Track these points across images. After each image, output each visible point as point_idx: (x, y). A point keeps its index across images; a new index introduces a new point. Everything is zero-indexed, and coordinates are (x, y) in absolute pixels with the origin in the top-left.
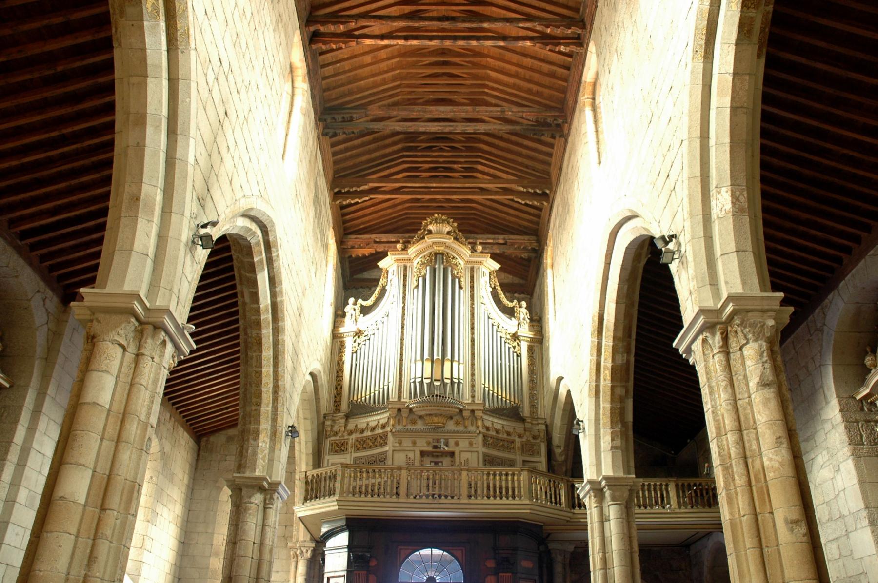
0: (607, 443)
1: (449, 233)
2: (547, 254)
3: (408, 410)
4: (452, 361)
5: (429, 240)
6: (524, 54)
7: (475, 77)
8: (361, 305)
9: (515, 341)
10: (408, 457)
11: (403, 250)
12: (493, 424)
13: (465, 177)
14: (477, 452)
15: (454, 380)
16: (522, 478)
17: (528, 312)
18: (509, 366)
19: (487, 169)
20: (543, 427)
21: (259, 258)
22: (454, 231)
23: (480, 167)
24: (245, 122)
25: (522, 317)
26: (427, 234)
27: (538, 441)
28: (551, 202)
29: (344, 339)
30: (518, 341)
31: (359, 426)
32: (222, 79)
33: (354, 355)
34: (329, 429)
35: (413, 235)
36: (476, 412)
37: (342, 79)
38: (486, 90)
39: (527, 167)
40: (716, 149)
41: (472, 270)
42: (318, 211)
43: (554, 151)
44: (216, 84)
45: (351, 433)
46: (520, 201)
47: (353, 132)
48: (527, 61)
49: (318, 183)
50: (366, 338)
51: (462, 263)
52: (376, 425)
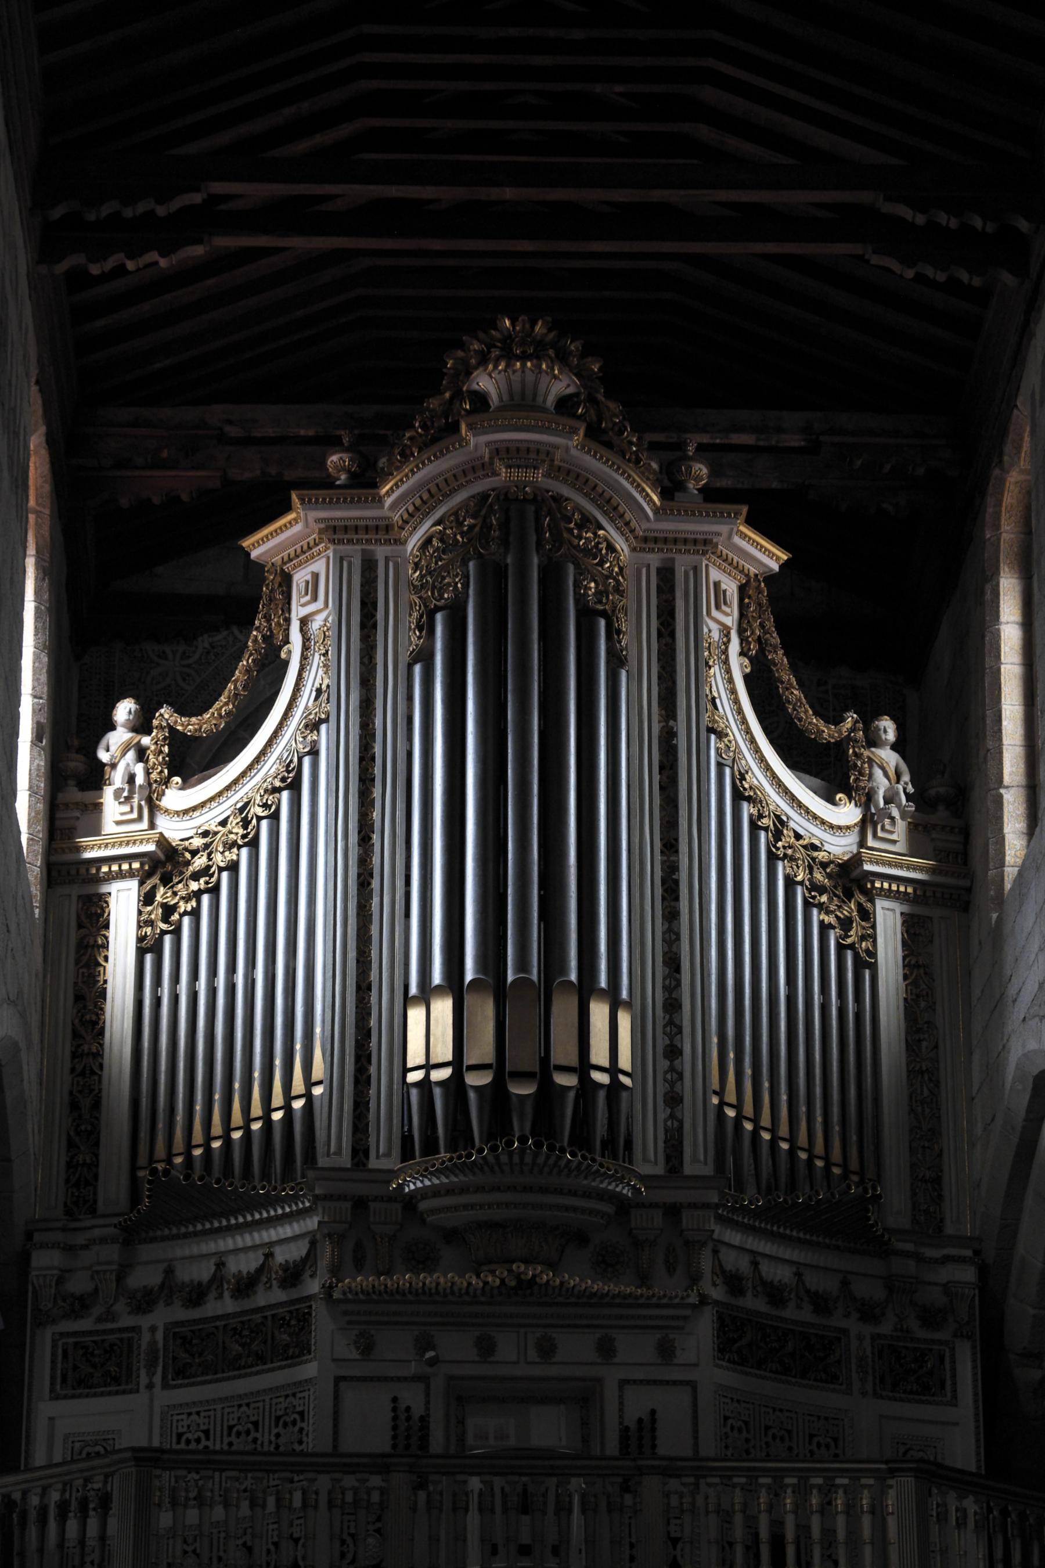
2: (999, 504)
4: (586, 990)
8: (172, 729)
9: (849, 895)
10: (403, 1406)
12: (755, 1264)
14: (693, 1385)
17: (904, 767)
18: (825, 1008)
20: (968, 1274)
22: (592, 400)
25: (881, 783)
29: (104, 889)
30: (862, 899)
33: (149, 958)
41: (666, 576)
50: (194, 886)
51: (621, 544)
52: (260, 1270)
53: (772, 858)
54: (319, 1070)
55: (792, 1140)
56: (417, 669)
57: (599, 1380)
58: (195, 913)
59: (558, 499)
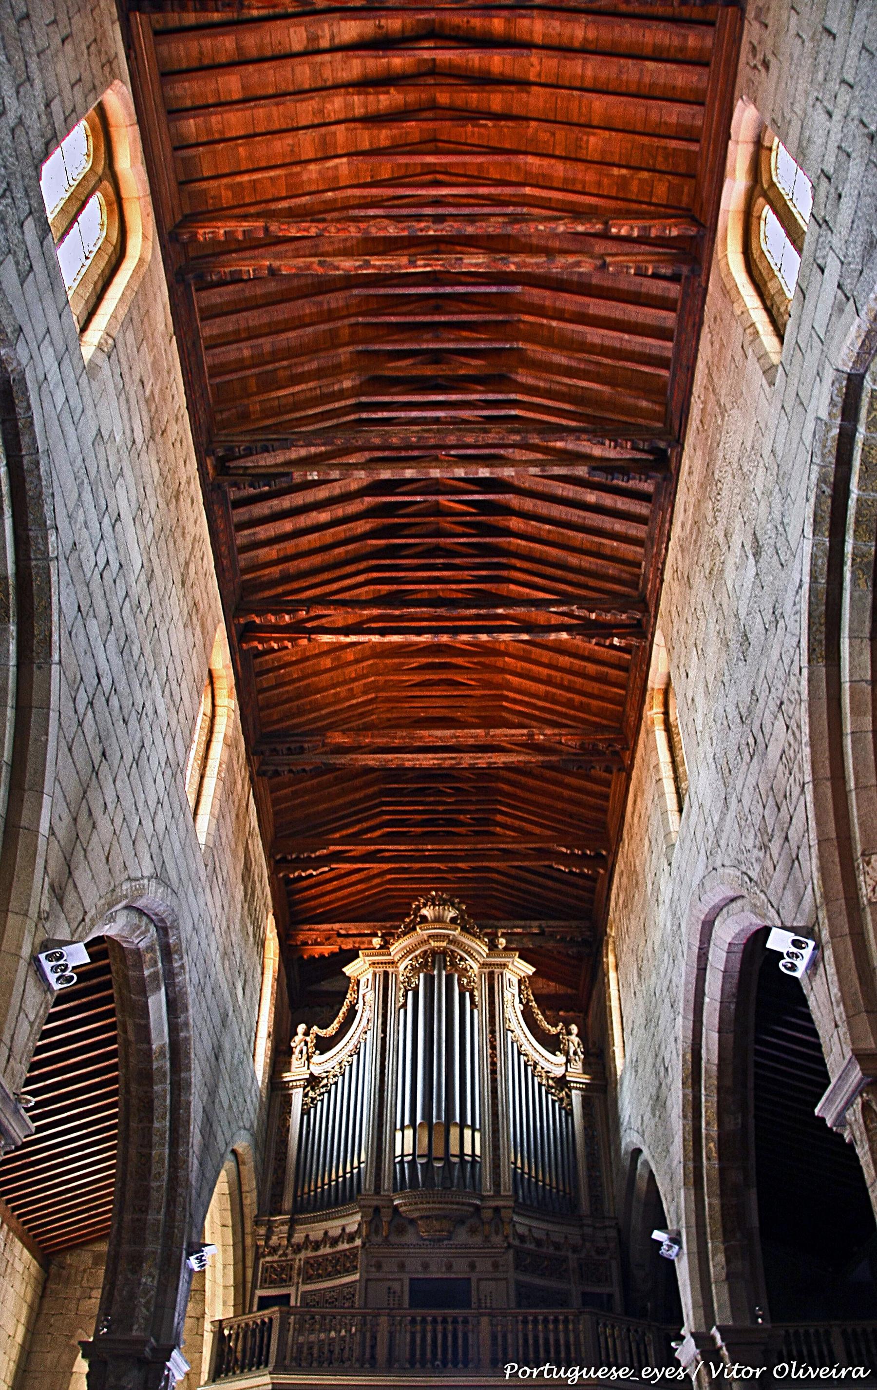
0: (719, 1267)
1: (453, 920)
3: (391, 1210)
4: (462, 1125)
5: (422, 933)
6: (559, 649)
7: (487, 685)
9: (562, 1090)
11: (382, 947)
13: (477, 833)
15: (467, 1158)
16: (581, 1327)
19: (509, 821)
20: (613, 1233)
21: (152, 970)
23: (499, 818)
24: (134, 765)
26: (420, 923)
27: (607, 1257)
28: (610, 866)
31: (311, 1238)
32: (100, 702)
33: (305, 1117)
34: (263, 1243)
35: (397, 923)
36: (503, 1210)
37: (287, 692)
38: (505, 704)
39: (571, 816)
40: (857, 794)
41: (491, 974)
42: (249, 892)
43: (611, 792)
44: (90, 711)
45: (298, 1249)
46: (563, 868)
47: (304, 770)
48: (564, 661)
49: (250, 847)
50: (323, 1090)
53: (533, 1076)
54: (363, 1158)
55: (543, 1181)
56: (402, 1011)
57: (469, 1279)
58: (322, 1101)
59: (452, 951)
